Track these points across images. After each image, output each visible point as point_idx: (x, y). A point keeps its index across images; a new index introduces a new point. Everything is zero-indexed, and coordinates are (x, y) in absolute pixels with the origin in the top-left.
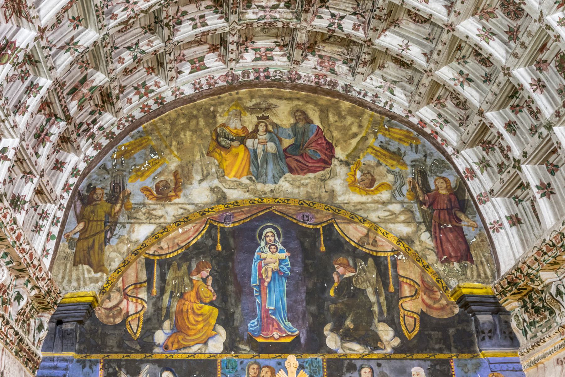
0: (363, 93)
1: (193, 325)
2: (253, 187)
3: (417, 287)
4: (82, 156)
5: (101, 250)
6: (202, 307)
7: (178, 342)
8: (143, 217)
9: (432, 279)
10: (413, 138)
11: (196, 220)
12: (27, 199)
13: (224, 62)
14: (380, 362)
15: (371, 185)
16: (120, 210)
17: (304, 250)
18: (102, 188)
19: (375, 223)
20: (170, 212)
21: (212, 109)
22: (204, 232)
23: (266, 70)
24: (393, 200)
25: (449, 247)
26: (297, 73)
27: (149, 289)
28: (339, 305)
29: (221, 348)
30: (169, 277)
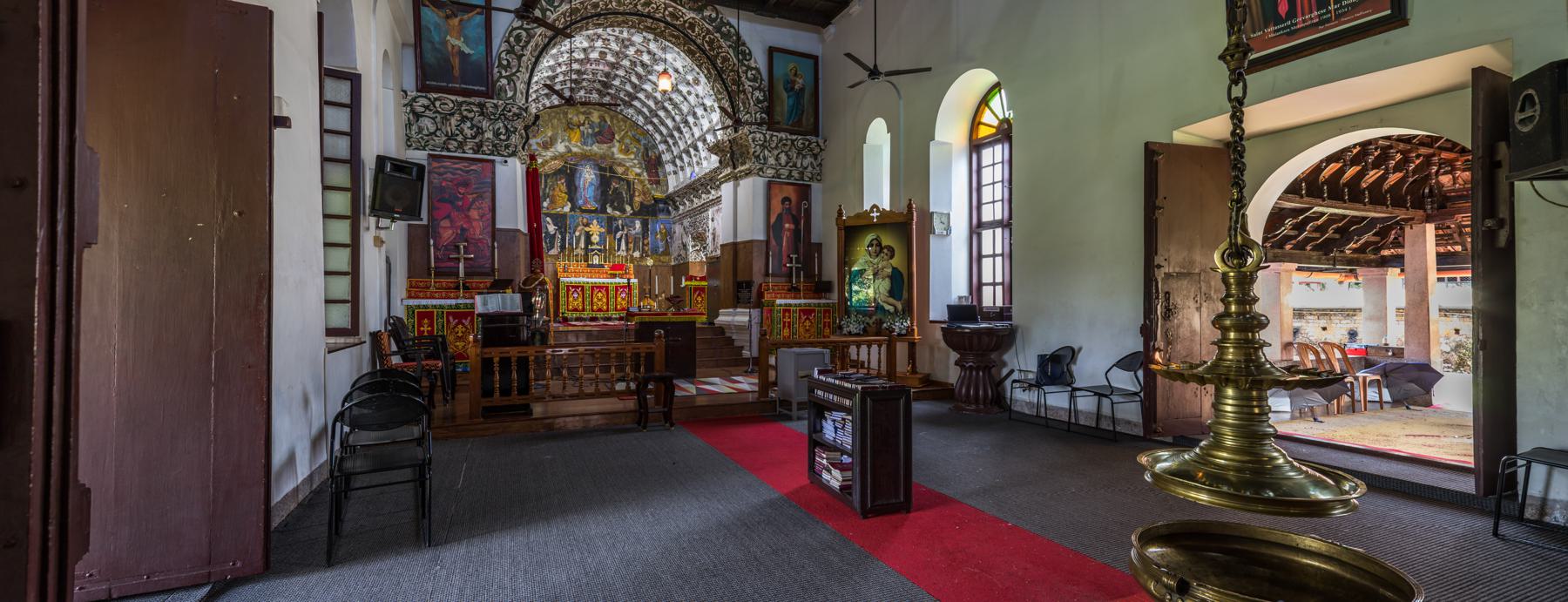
20: (549, 154)
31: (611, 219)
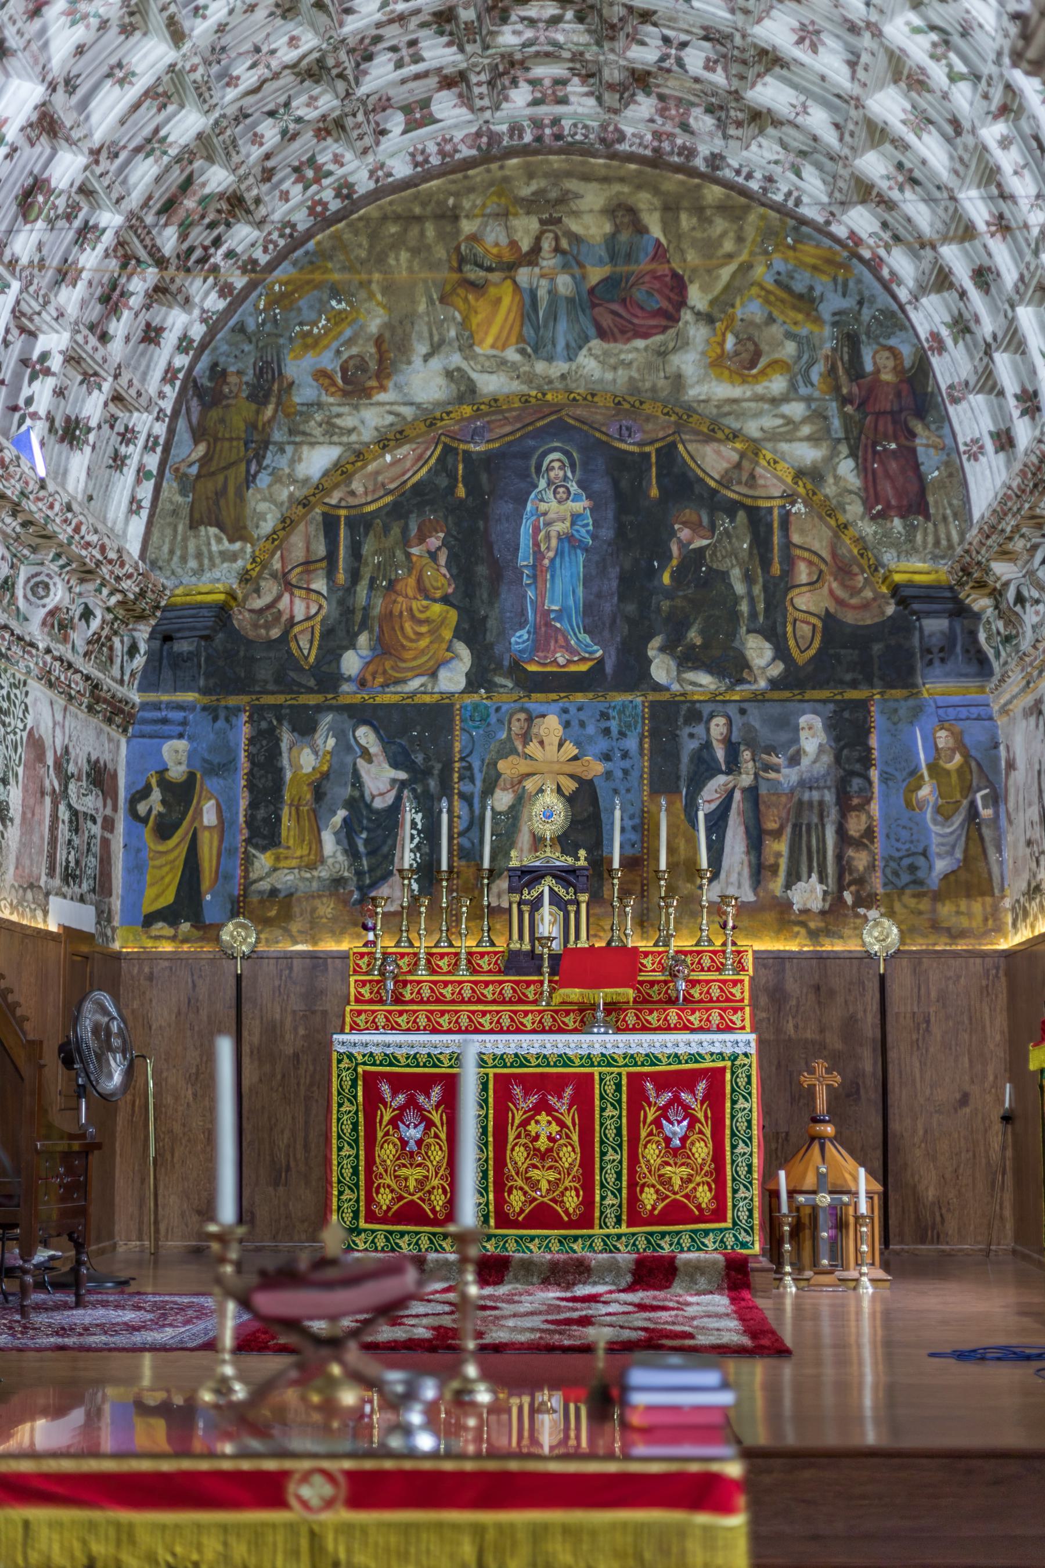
0: (745, 171)
1: (412, 641)
2: (527, 368)
3: (823, 567)
4: (196, 312)
5: (241, 497)
6: (427, 608)
7: (385, 672)
8: (318, 432)
9: (850, 551)
10: (840, 265)
11: (418, 436)
12: (93, 423)
13: (472, 109)
14: (745, 705)
15: (753, 364)
16: (274, 417)
17: (619, 495)
18: (240, 373)
19: (754, 441)
20: (369, 420)
21: (451, 201)
22: (433, 461)
23: (556, 122)
24: (792, 395)
25: (887, 489)
26: (617, 130)
27: (331, 574)
28: (679, 602)
29: (461, 683)
30: (366, 549)
31: (670, 717)
